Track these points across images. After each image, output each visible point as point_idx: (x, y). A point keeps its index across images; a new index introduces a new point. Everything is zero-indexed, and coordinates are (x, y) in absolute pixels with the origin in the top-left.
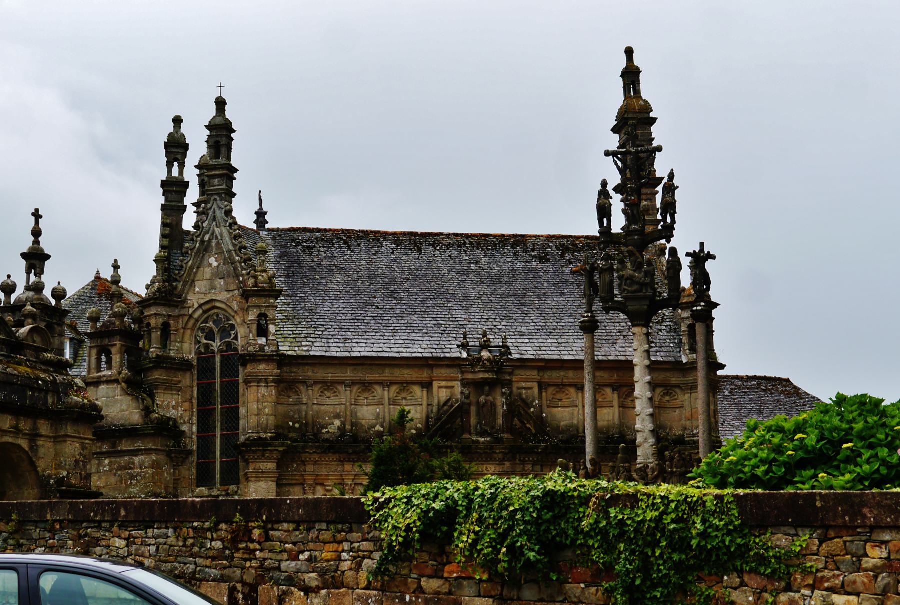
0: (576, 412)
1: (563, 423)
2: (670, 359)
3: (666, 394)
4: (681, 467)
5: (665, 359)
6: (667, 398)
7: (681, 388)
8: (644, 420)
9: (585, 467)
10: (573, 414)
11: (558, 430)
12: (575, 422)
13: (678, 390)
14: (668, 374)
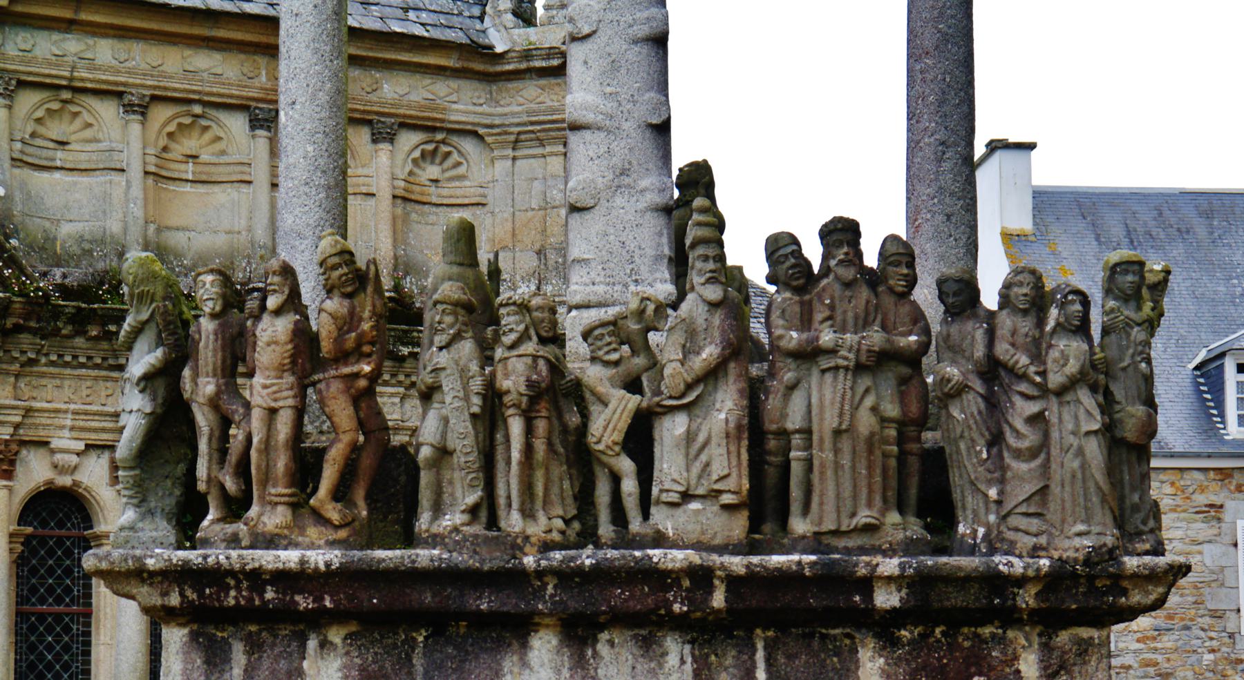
0: (118, 193)
1: (66, 230)
2: (451, 35)
3: (429, 156)
4: (863, 323)
5: (436, 34)
6: (433, 171)
7: (480, 138)
8: (614, 66)
9: (293, 301)
10: (106, 197)
11: (45, 248)
12: (115, 227)
13: (468, 145)
14: (442, 89)
